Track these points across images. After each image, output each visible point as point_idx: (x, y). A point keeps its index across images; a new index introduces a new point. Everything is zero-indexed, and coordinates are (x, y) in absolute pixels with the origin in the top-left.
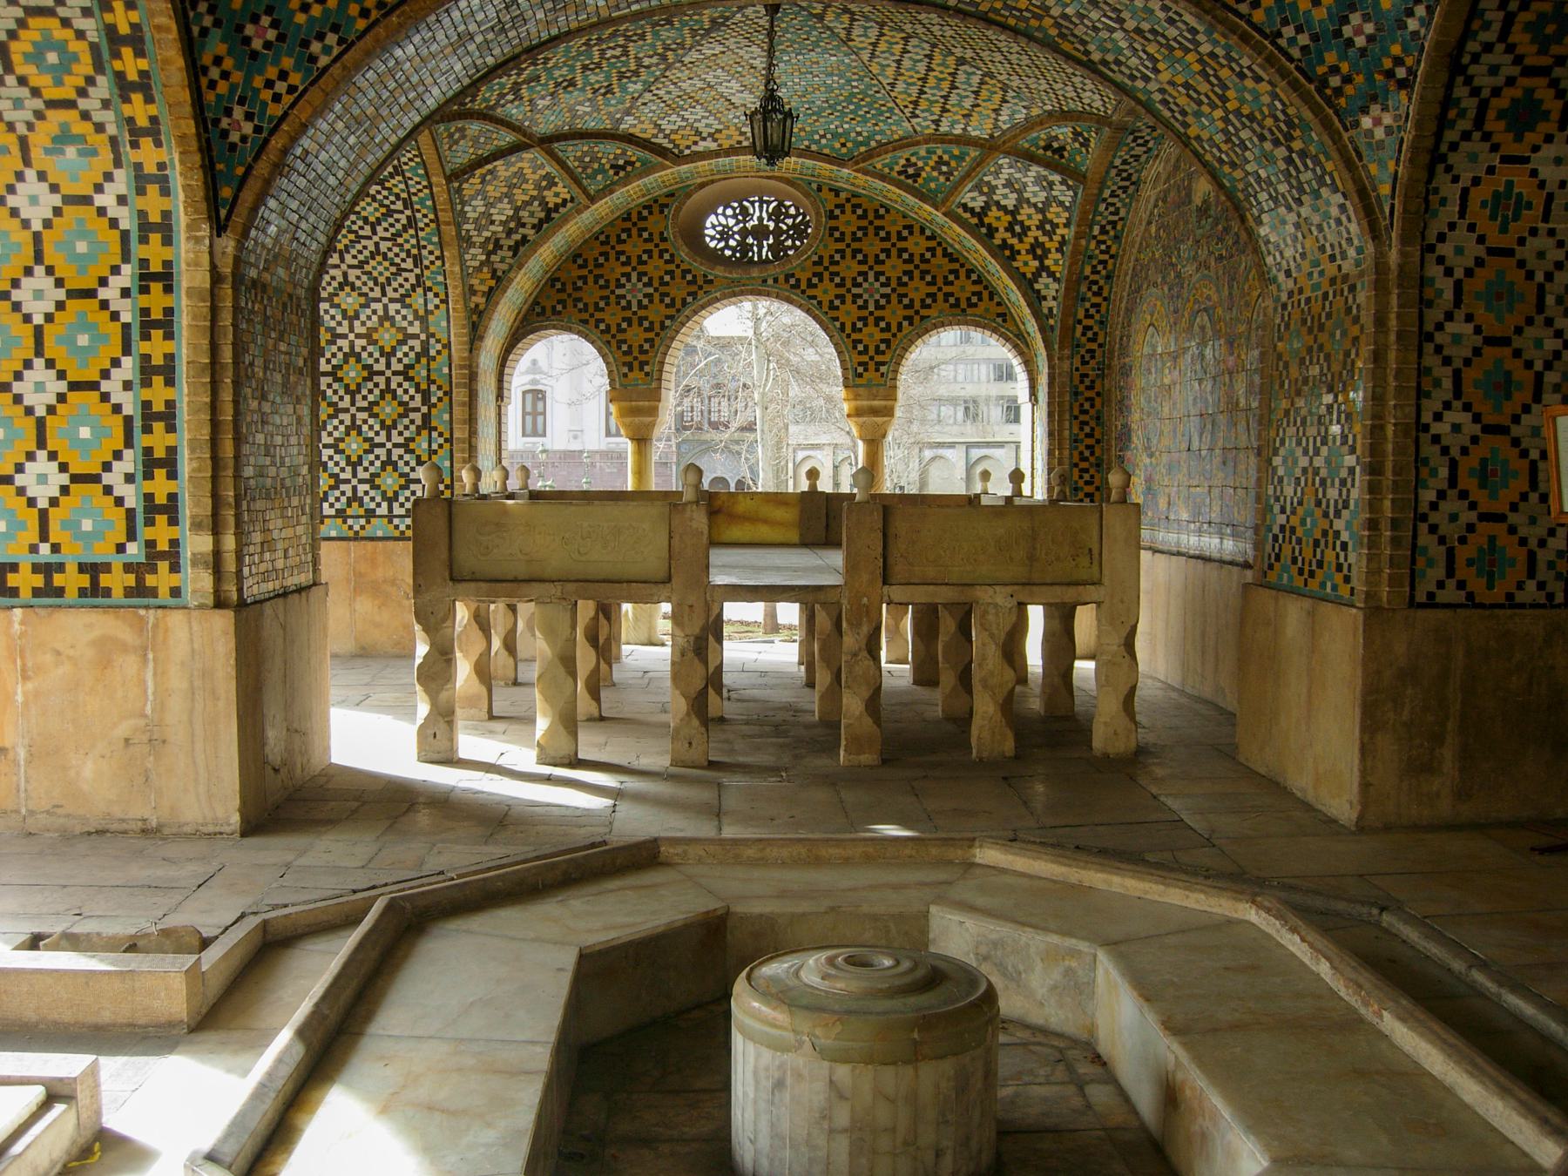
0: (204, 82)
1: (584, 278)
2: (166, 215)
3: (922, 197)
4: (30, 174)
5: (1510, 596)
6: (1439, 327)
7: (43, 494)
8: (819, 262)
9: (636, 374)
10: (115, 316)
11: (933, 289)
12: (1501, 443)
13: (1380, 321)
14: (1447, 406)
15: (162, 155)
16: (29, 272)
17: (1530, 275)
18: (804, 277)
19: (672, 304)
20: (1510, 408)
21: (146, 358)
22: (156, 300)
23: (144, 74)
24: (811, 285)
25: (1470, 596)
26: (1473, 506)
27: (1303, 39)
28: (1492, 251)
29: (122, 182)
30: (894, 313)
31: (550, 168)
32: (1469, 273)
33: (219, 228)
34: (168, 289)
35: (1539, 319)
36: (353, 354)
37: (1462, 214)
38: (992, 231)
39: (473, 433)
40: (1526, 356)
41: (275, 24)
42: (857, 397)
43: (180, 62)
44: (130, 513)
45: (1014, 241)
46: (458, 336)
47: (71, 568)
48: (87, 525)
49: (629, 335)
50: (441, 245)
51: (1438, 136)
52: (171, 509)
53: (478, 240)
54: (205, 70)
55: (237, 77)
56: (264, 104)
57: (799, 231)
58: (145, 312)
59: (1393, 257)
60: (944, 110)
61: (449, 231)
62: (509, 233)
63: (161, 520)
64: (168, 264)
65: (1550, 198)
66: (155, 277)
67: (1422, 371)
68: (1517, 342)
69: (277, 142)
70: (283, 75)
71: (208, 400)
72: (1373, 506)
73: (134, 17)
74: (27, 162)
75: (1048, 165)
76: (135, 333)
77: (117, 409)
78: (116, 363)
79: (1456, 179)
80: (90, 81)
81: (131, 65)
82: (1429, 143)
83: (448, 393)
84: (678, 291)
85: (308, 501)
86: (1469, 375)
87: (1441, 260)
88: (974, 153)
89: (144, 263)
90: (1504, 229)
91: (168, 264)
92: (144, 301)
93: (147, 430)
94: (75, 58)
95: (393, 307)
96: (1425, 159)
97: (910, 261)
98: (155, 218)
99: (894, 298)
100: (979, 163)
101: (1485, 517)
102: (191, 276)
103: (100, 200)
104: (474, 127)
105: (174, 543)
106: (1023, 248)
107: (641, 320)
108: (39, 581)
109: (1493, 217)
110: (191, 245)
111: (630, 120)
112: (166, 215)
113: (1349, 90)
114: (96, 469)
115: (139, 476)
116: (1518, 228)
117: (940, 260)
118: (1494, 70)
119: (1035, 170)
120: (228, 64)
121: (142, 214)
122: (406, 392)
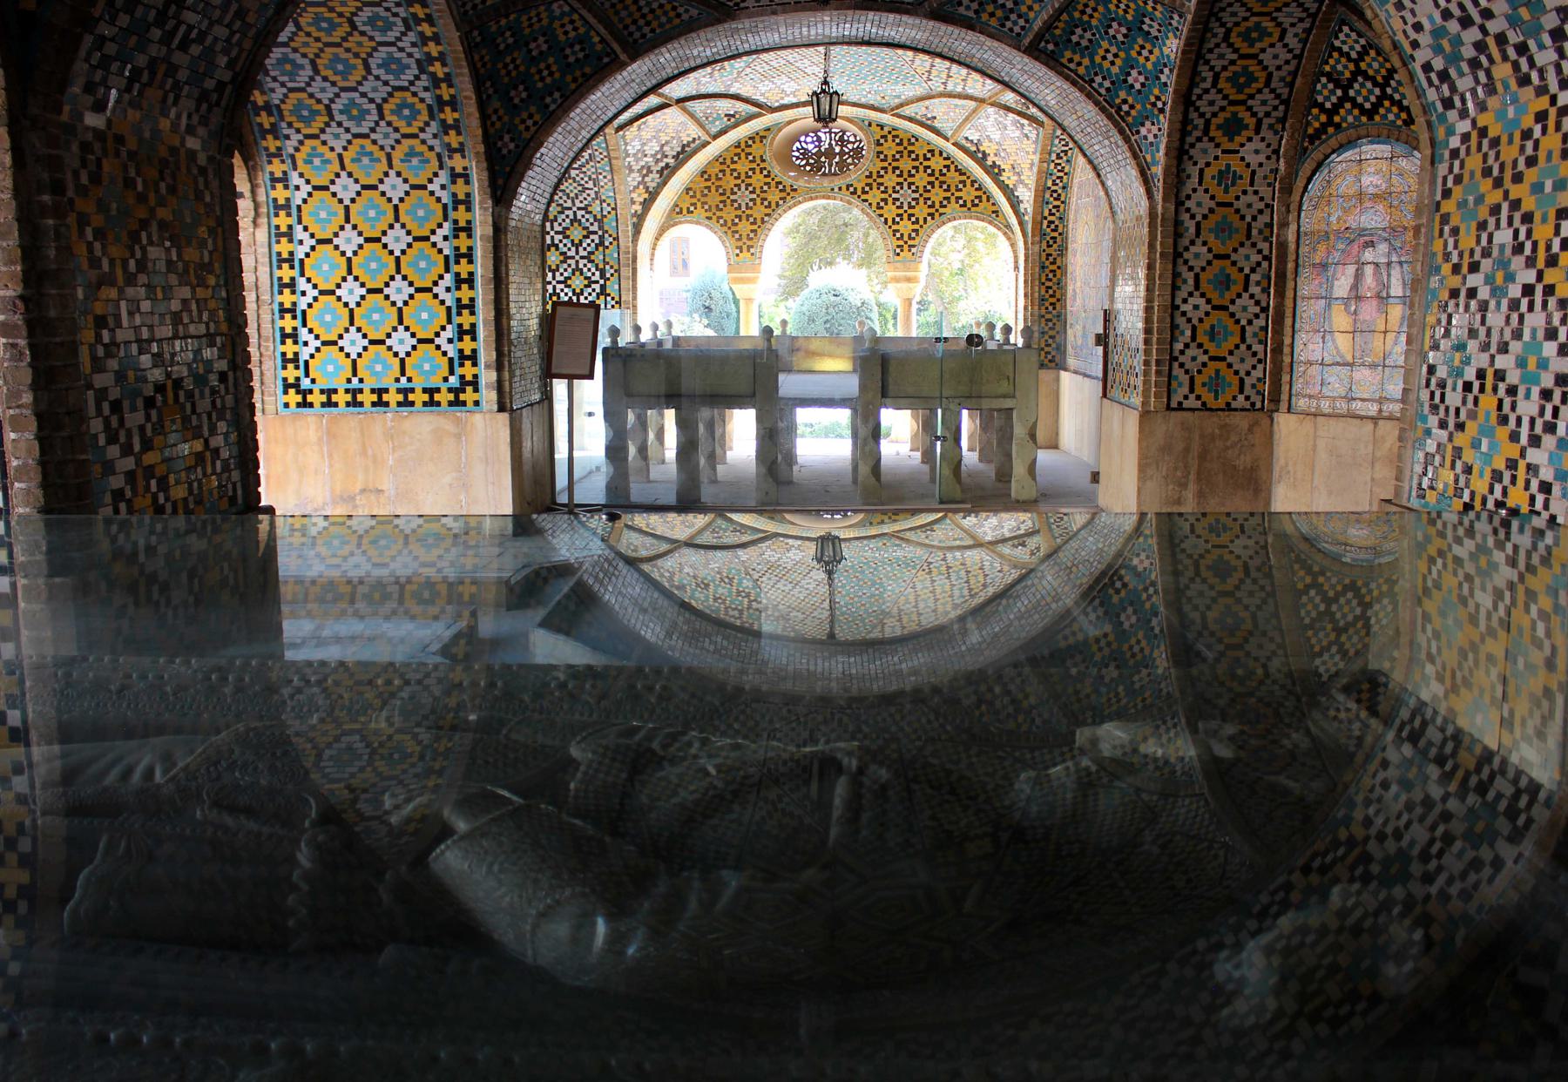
2: (468, 195)
4: (392, 173)
5: (1228, 404)
6: (1187, 249)
8: (869, 176)
9: (745, 254)
12: (1223, 315)
13: (1151, 246)
14: (1191, 294)
15: (466, 163)
17: (1243, 218)
19: (769, 206)
20: (1228, 296)
21: (458, 274)
22: (463, 243)
23: (456, 120)
24: (864, 192)
25: (1204, 404)
26: (1206, 352)
27: (1107, 84)
28: (1219, 204)
29: (443, 177)
30: (921, 211)
32: (1205, 217)
34: (470, 236)
35: (1248, 243)
37: (1200, 183)
38: (985, 155)
39: (635, 298)
40: (1239, 265)
44: (451, 360)
46: (626, 229)
47: (419, 390)
48: (427, 367)
51: (1182, 140)
52: (474, 358)
53: (636, 168)
54: (489, 117)
55: (506, 119)
58: (457, 249)
60: (949, 77)
62: (657, 161)
65: (1253, 173)
66: (462, 229)
67: (1176, 275)
68: (1234, 257)
70: (531, 116)
72: (1147, 352)
73: (452, 91)
74: (391, 167)
75: (1020, 114)
79: (1195, 164)
81: (449, 116)
82: (1177, 144)
84: (774, 196)
86: (1203, 276)
87: (1188, 210)
88: (972, 104)
89: (456, 222)
90: (1226, 191)
91: (469, 222)
92: (456, 243)
93: (459, 314)
94: (419, 112)
95: (580, 213)
96: (1174, 153)
98: (461, 197)
99: (921, 201)
101: (1212, 359)
105: (475, 376)
107: (748, 217)
108: (400, 398)
109: (1219, 184)
111: (737, 85)
112: (468, 195)
113: (1133, 113)
114: (431, 336)
116: (1234, 191)
117: (952, 173)
118: (1211, 103)
119: (1011, 116)
120: (501, 112)
121: (454, 195)
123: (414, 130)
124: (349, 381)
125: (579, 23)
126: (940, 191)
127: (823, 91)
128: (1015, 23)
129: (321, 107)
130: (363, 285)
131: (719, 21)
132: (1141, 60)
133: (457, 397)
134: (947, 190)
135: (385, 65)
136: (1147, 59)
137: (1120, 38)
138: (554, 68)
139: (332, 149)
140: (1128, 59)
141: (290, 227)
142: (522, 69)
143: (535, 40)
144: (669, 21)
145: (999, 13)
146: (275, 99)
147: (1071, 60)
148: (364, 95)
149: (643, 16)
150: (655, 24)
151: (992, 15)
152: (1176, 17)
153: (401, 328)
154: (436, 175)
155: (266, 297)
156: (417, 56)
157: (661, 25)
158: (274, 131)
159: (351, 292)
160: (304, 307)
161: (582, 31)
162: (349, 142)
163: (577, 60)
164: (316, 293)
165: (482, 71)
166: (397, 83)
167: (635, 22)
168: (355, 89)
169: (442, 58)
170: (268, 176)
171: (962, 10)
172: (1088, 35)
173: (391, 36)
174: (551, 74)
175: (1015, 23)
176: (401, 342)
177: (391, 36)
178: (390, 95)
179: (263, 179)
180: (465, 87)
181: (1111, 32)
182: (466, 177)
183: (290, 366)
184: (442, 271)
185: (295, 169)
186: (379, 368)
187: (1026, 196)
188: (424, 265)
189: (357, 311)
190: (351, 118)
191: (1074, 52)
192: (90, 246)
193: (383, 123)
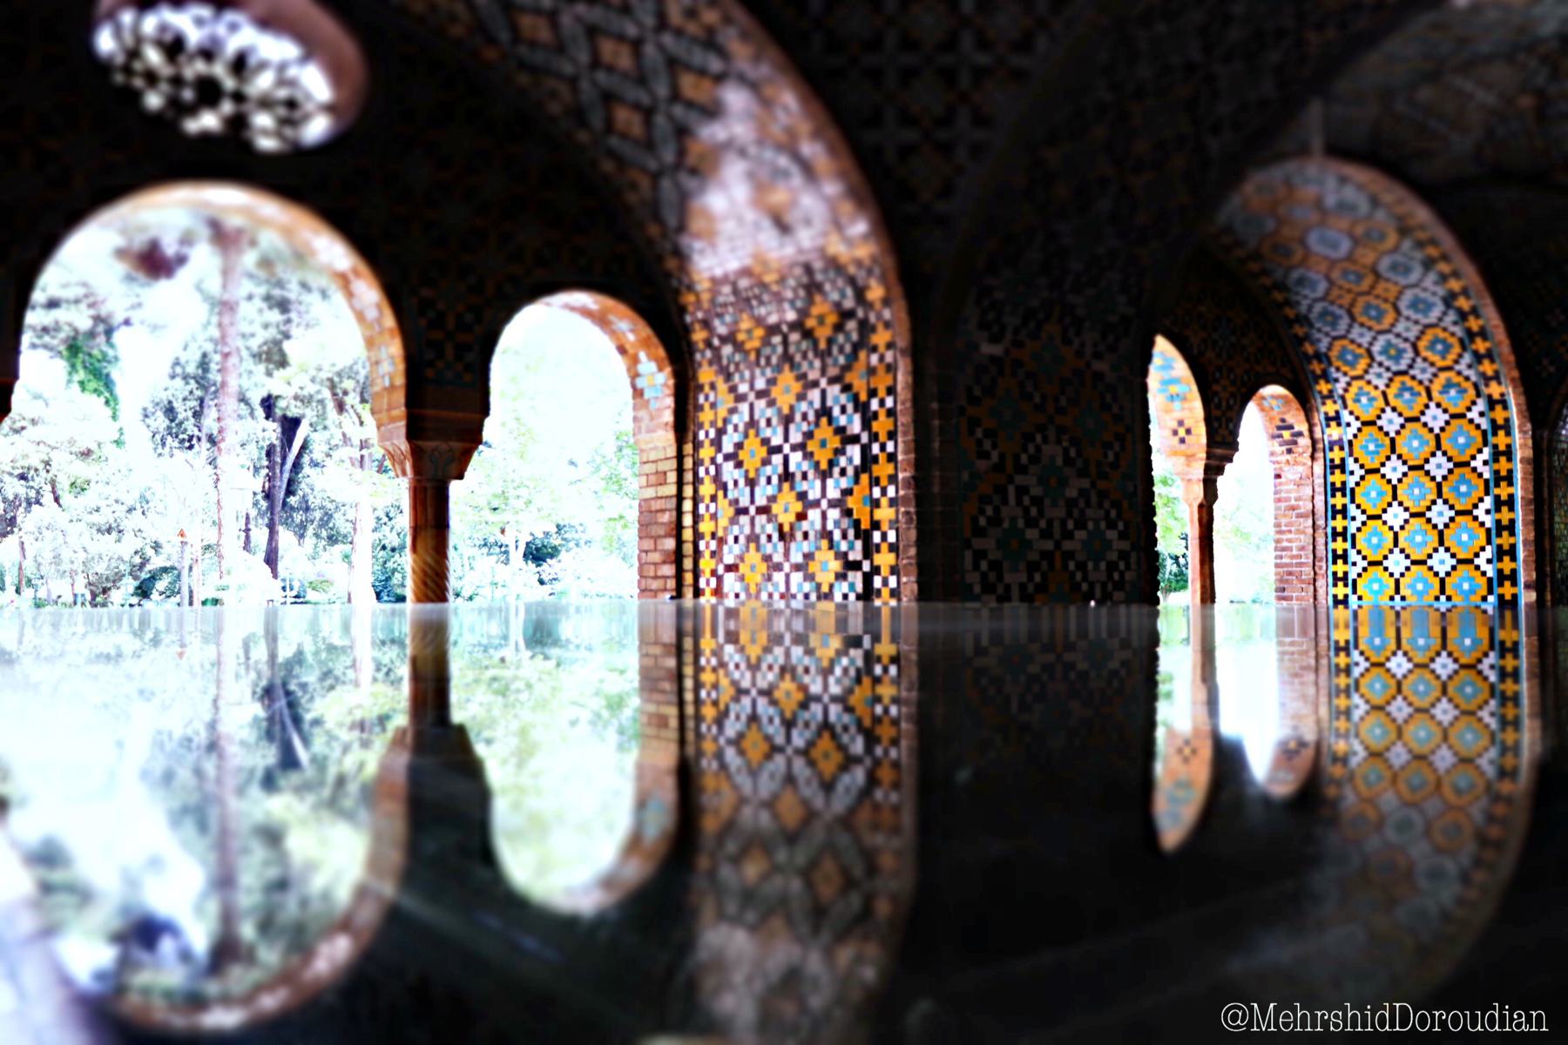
4: (1432, 405)
10: (1480, 475)
15: (1503, 389)
16: (1433, 455)
29: (1481, 405)
52: (1513, 577)
64: (1509, 446)
71: (1532, 518)
73: (1481, 322)
74: (1430, 398)
76: (1492, 484)
77: (1482, 524)
80: (1460, 356)
81: (1481, 346)
98: (1500, 422)
103: (1470, 415)
105: (1515, 596)
110: (1521, 435)
112: (1507, 420)
115: (1495, 560)
121: (1493, 422)
123: (1448, 362)
124: (1392, 598)
129: (1361, 351)
135: (1414, 305)
139: (1376, 388)
141: (1343, 460)
146: (1323, 346)
148: (1398, 335)
155: (1321, 522)
158: (1325, 376)
160: (1354, 531)
164: (1364, 518)
169: (1465, 292)
170: (1322, 417)
176: (1441, 561)
177: (1414, 276)
178: (1422, 332)
179: (1319, 418)
180: (1491, 317)
182: (1504, 404)
183: (1340, 584)
184: (1481, 494)
185: (1345, 407)
188: (1465, 491)
189: (1402, 535)
190: (1390, 358)
192: (979, 443)
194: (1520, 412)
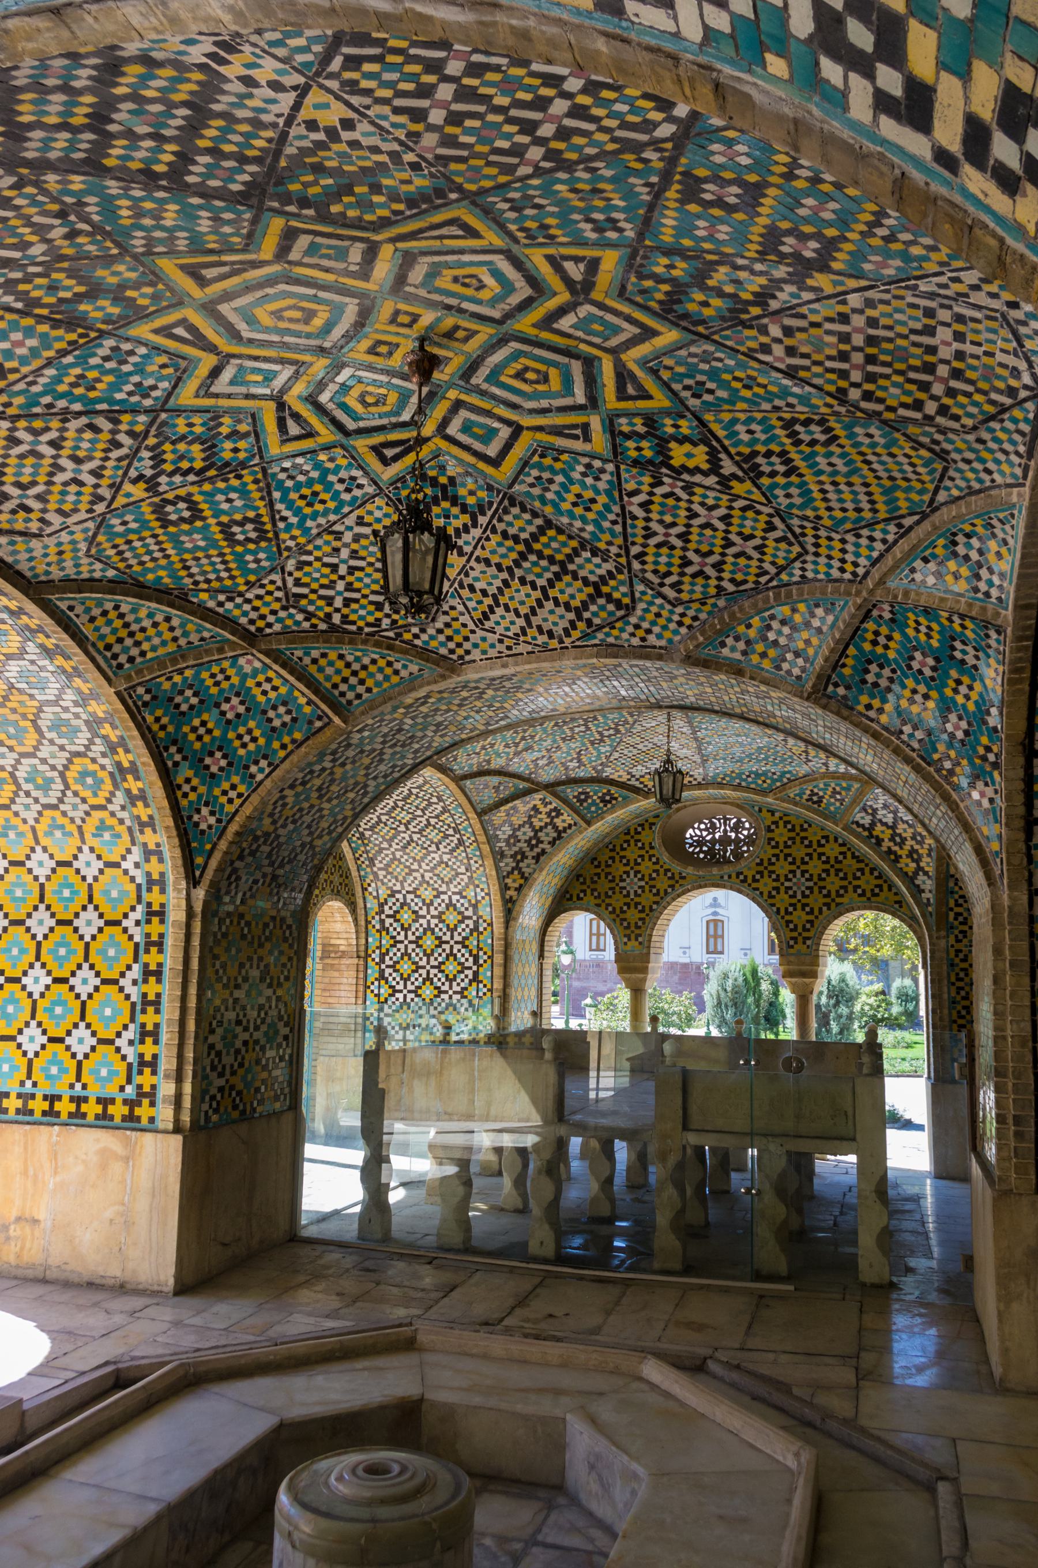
0: (179, 794)
1: (598, 875)
2: (162, 874)
3: (826, 817)
7: (80, 1050)
9: (633, 943)
11: (845, 883)
18: (750, 874)
19: (657, 894)
22: (155, 928)
24: (755, 880)
29: (136, 855)
30: (816, 901)
31: (555, 803)
33: (193, 881)
36: (429, 929)
38: (879, 841)
39: (506, 985)
41: (225, 756)
42: (789, 963)
43: (160, 784)
45: (896, 848)
47: (92, 1100)
48: (104, 1072)
49: (628, 915)
50: (481, 856)
52: (153, 1064)
54: (179, 787)
56: (222, 806)
57: (750, 841)
58: (148, 935)
59: (1005, 899)
61: (486, 848)
63: (147, 1071)
69: (233, 828)
70: (234, 787)
77: (128, 997)
78: (129, 968)
80: (113, 794)
81: (134, 786)
82: (1021, 810)
83: (491, 957)
85: (289, 1051)
91: (162, 905)
92: (147, 928)
95: (455, 898)
96: (1020, 823)
97: (827, 862)
98: (156, 876)
100: (861, 793)
102: (176, 914)
104: (495, 780)
105: (154, 1087)
106: (903, 853)
107: (637, 904)
112: (162, 874)
117: (849, 861)
120: (195, 782)
121: (149, 874)
122: (464, 956)
124: (22, 1084)
125: (277, 682)
126: (837, 880)
127: (666, 770)
128: (793, 664)
130: (49, 973)
131: (444, 677)
132: (960, 699)
133: (132, 1111)
134: (845, 878)
136: (967, 697)
137: (928, 672)
138: (257, 733)
140: (943, 698)
142: (217, 733)
143: (228, 700)
144: (387, 678)
145: (772, 653)
147: (869, 707)
148: (44, 761)
149: (355, 673)
150: (370, 683)
151: (763, 655)
152: (994, 635)
153: (82, 1025)
154: (129, 851)
156: (84, 716)
157: (378, 684)
159: (36, 980)
161: (283, 690)
162: (40, 813)
163: (284, 724)
165: (162, 734)
166: (74, 748)
167: (345, 680)
168: (32, 755)
171: (725, 652)
172: (886, 672)
173: (50, 694)
174: (254, 740)
175: (793, 664)
180: (139, 754)
181: (916, 665)
186: (54, 1070)
187: (927, 884)
189: (41, 1004)
190: (38, 788)
191: (872, 696)
193: (69, 793)
194: (175, 867)
